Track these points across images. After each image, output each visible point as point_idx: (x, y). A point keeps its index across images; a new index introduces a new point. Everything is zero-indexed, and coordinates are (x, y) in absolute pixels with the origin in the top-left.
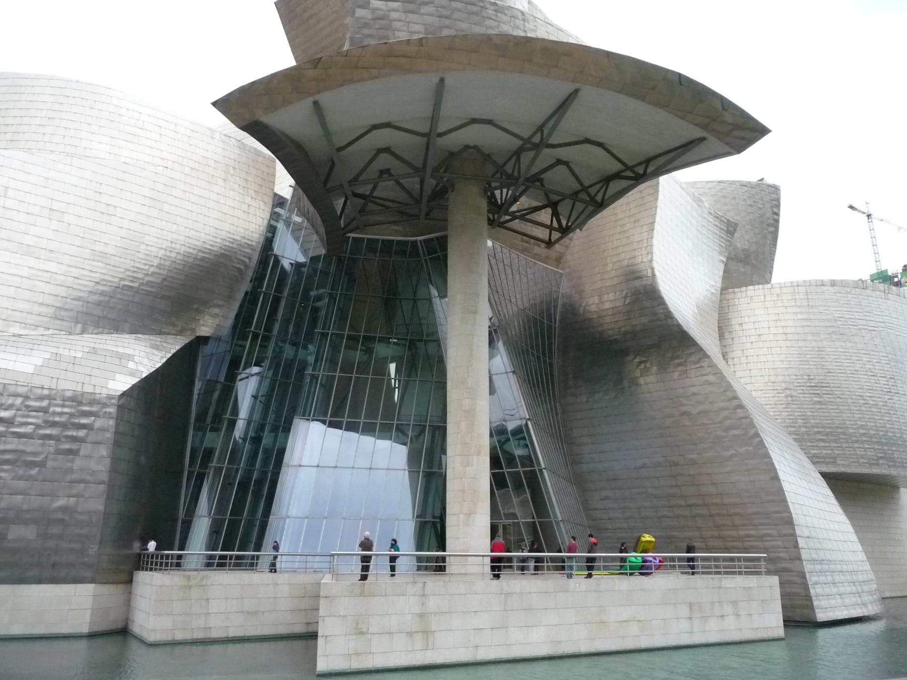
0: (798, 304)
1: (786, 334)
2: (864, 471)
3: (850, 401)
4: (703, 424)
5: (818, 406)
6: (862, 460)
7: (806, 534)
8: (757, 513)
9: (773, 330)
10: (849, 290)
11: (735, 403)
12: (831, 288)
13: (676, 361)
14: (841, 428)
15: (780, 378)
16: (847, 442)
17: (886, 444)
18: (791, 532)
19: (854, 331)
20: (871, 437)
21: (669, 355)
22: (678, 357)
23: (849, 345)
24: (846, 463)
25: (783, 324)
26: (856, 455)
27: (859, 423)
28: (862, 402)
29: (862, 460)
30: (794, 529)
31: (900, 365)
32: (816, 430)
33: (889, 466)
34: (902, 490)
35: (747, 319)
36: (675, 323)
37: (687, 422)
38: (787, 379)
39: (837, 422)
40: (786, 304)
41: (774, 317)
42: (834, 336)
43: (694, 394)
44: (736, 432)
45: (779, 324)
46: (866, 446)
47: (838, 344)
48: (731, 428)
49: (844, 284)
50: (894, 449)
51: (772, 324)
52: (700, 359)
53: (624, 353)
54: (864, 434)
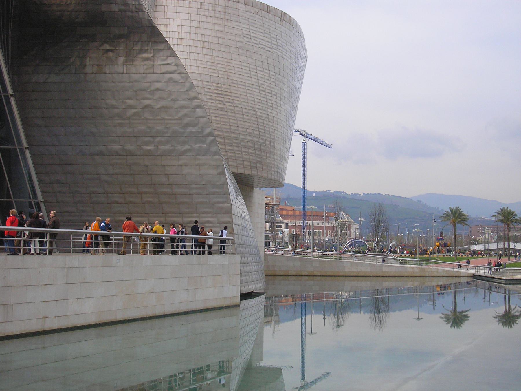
0: (217, 15)
1: (204, 42)
3: (244, 110)
4: (163, 119)
5: (221, 112)
6: (246, 163)
7: (237, 223)
8: (202, 203)
9: (193, 37)
10: (257, 10)
11: (196, 103)
12: (244, 6)
13: (145, 55)
14: (235, 133)
16: (237, 147)
18: (229, 219)
19: (255, 49)
21: (137, 48)
22: (146, 51)
23: (250, 60)
24: (235, 164)
25: (203, 31)
26: (243, 158)
27: (248, 131)
28: (252, 112)
29: (246, 163)
30: (232, 218)
31: (282, 84)
34: (256, 190)
35: (171, 22)
36: (146, 17)
37: (147, 115)
39: (232, 128)
40: (207, 14)
41: (195, 24)
42: (241, 51)
43: (158, 90)
44: (194, 130)
45: (199, 31)
46: (250, 151)
47: (243, 58)
48: (187, 125)
51: (193, 30)
52: (168, 57)
53: (93, 37)
54: (250, 141)
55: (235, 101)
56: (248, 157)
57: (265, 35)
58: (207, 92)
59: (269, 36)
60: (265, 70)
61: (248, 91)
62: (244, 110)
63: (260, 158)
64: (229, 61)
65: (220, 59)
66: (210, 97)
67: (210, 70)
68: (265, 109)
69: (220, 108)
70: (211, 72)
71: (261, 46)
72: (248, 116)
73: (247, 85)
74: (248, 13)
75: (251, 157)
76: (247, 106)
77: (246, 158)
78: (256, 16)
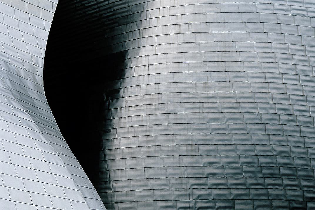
14: (246, 157)
15: (163, 88)
19: (282, 18)
20: (297, 169)
26: (268, 195)
32: (206, 160)
38: (172, 88)
42: (250, 26)
46: (286, 182)
54: (285, 165)
55: (242, 105)
56: (282, 192)
58: (186, 98)
60: (308, 48)
61: (271, 85)
62: (265, 117)
64: (227, 44)
65: (211, 44)
66: (191, 106)
67: (191, 65)
69: (212, 119)
70: (193, 67)
73: (268, 75)
75: (289, 193)
76: (271, 108)
77: (277, 195)
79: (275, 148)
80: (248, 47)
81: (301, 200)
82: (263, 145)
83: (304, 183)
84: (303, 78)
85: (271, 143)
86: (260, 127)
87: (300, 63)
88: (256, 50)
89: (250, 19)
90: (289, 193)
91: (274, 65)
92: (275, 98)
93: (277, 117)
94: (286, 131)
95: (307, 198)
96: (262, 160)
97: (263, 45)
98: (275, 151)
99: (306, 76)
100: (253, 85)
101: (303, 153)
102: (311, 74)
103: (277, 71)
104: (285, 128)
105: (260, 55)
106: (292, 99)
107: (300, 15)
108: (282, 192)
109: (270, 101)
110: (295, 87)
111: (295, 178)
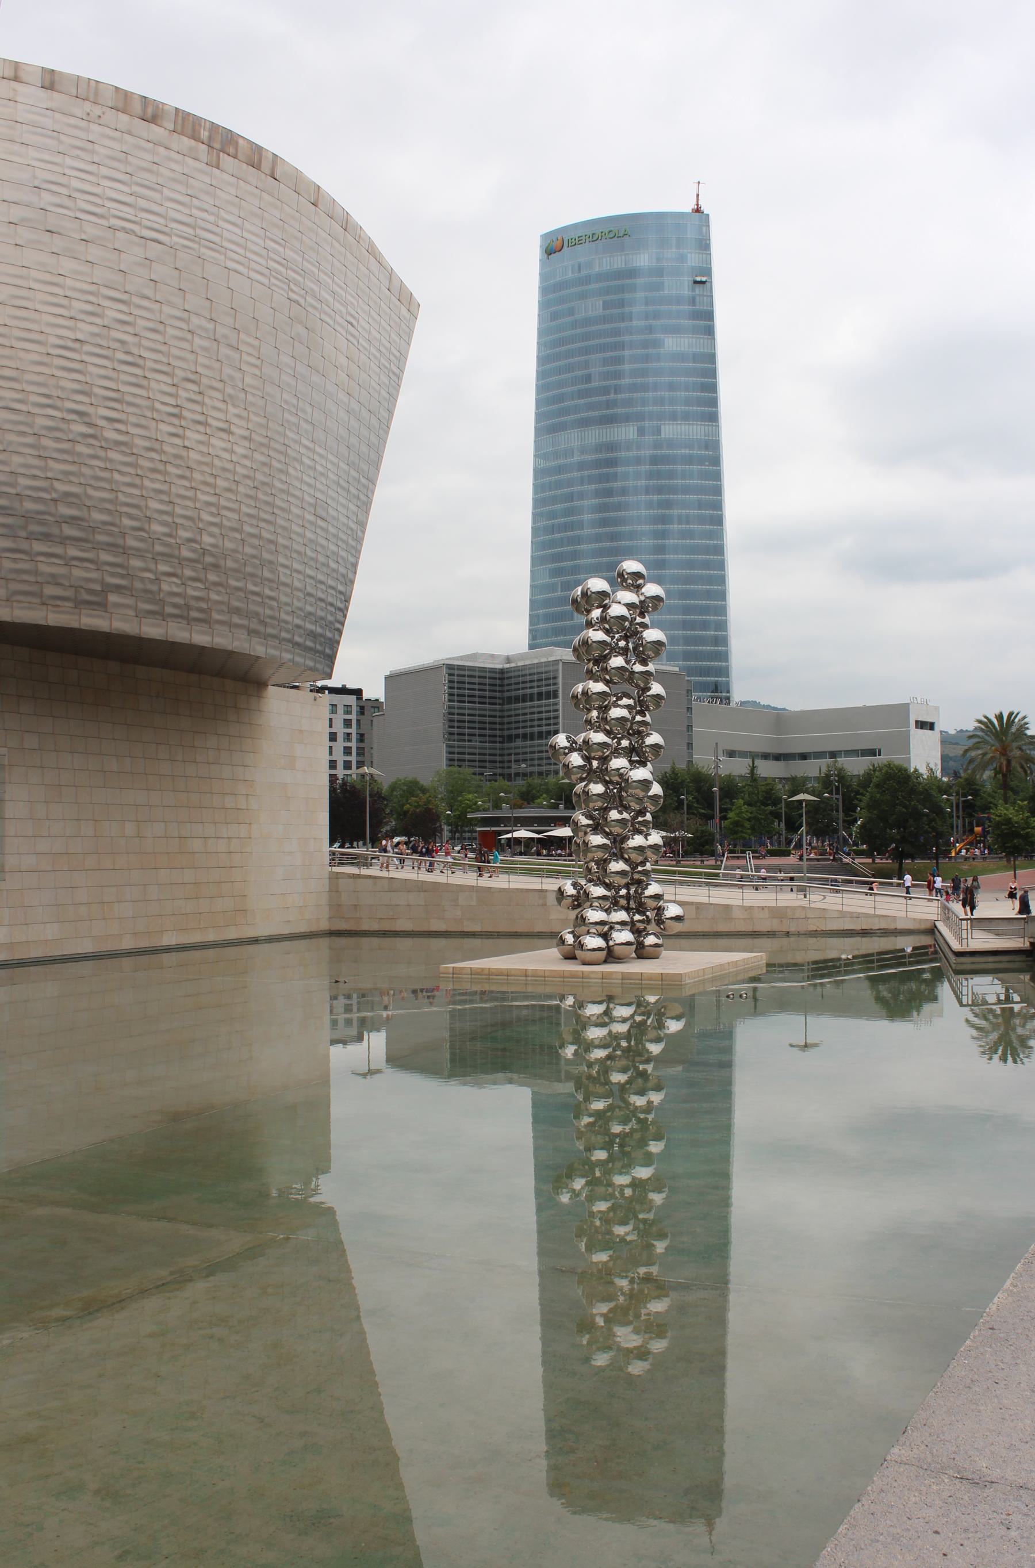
2: (53, 618)
6: (50, 590)
10: (97, 111)
17: (140, 554)
19: (91, 231)
20: (93, 529)
23: (68, 265)
26: (36, 573)
28: (79, 428)
29: (50, 590)
33: (140, 615)
34: (271, 690)
42: (24, 234)
46: (73, 552)
49: (88, 91)
50: (163, 568)
54: (73, 520)
56: (63, 570)
57: (135, 188)
59: (156, 196)
60: (136, 300)
63: (122, 576)
68: (143, 422)
71: (113, 222)
72: (58, 440)
74: (57, 116)
75: (77, 573)
77: (53, 575)
78: (94, 127)
79: (57, 485)
80: (16, 276)
81: (98, 588)
82: (35, 477)
83: (105, 557)
84: (120, 356)
85: (49, 475)
86: (30, 440)
87: (118, 326)
88: (33, 285)
89: (24, 220)
90: (77, 573)
91: (70, 323)
92: (63, 389)
93: (63, 426)
94: (80, 454)
95: (108, 585)
96: (29, 505)
97: (48, 278)
98: (56, 491)
99: (127, 353)
100: (21, 354)
101: (110, 501)
102: (135, 351)
103: (72, 335)
104: (79, 448)
105: (40, 296)
106: (96, 395)
107: (126, 231)
108: (63, 570)
109: (54, 393)
110: (103, 372)
111: (90, 545)
